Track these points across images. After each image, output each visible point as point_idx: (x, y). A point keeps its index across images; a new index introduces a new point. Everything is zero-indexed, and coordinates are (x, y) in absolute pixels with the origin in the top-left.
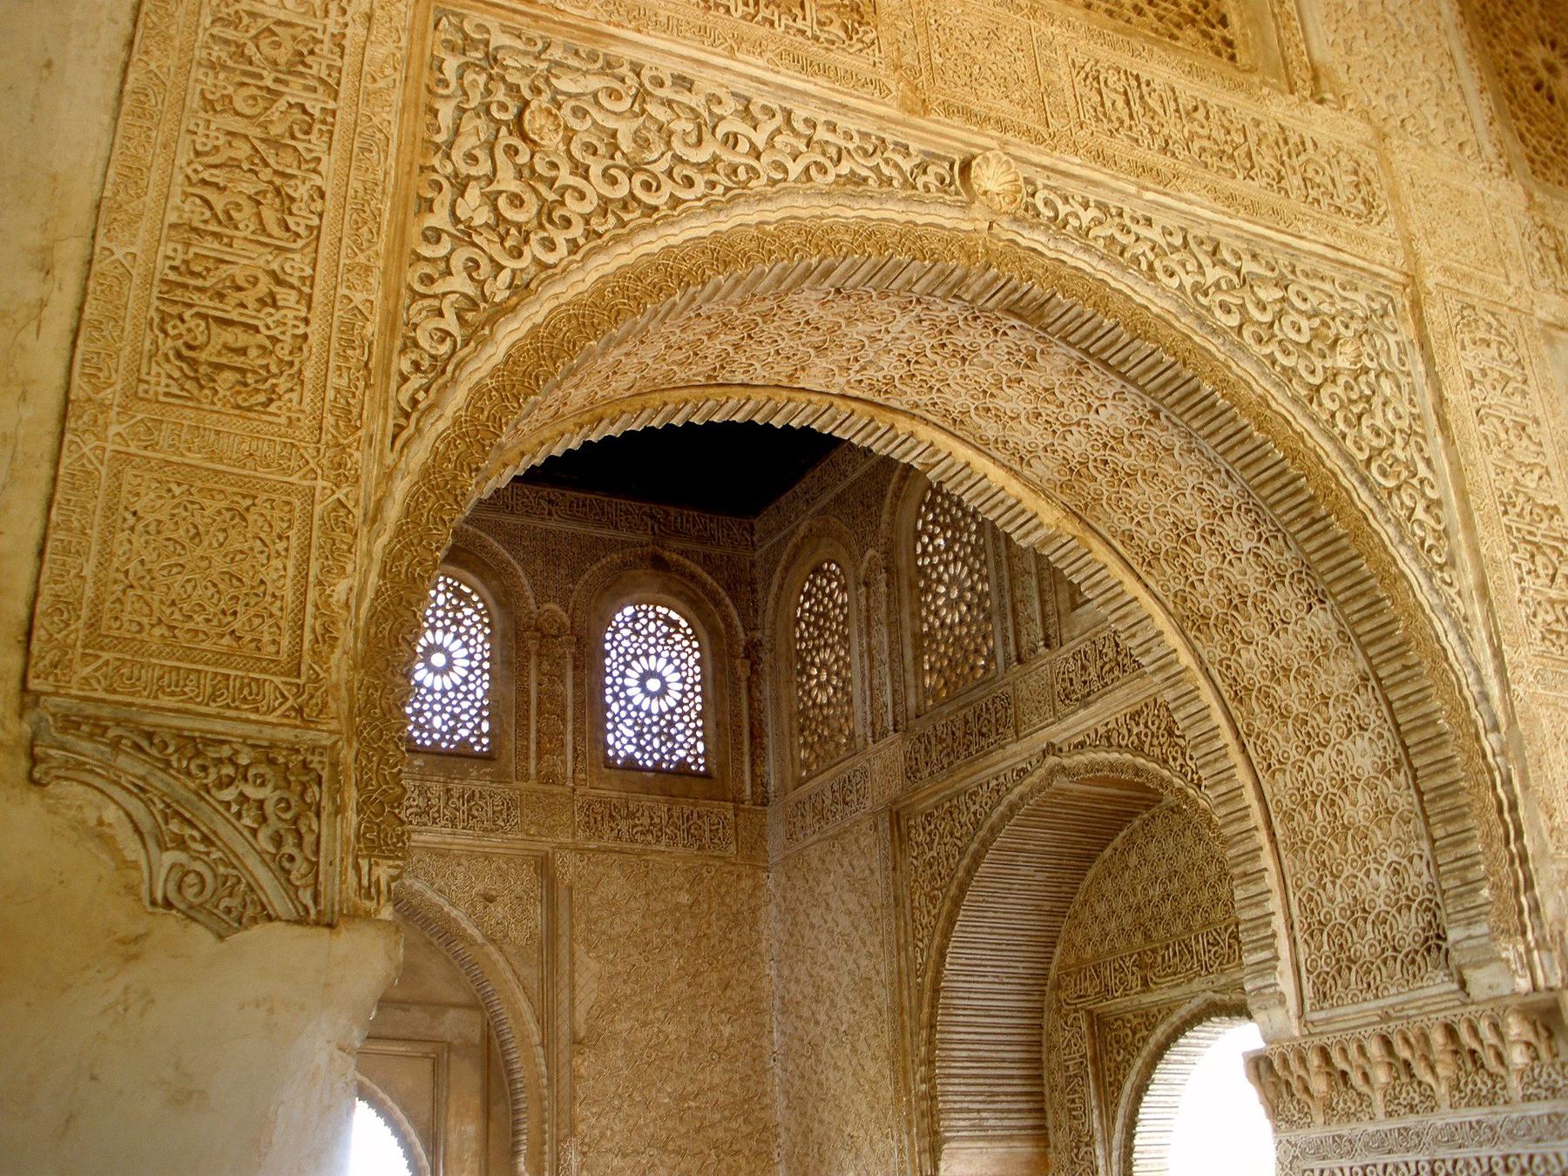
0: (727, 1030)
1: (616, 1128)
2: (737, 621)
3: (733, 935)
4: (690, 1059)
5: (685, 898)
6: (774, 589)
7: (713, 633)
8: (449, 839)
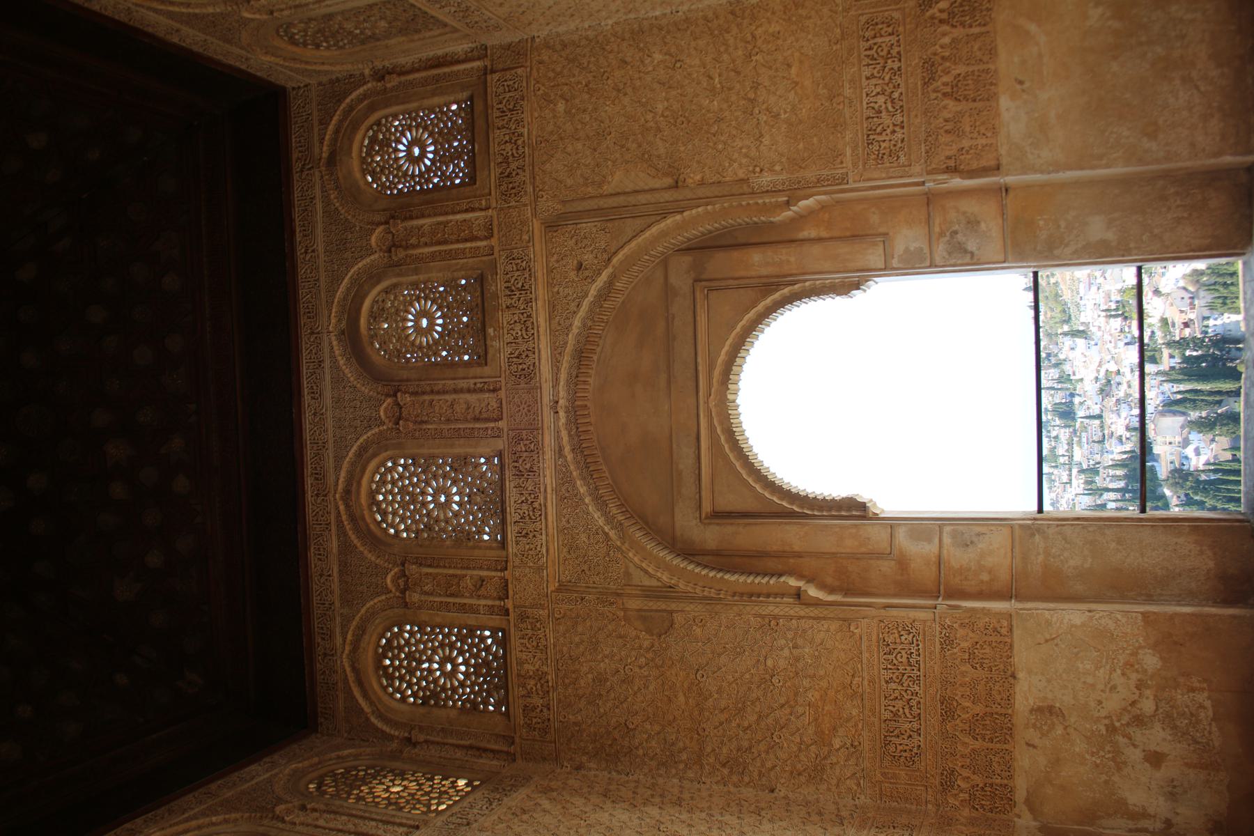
0: (658, 57)
1: (740, 144)
2: (361, 90)
3: (585, 61)
4: (682, 87)
5: (561, 107)
6: (326, 68)
7: (372, 108)
8: (540, 303)
